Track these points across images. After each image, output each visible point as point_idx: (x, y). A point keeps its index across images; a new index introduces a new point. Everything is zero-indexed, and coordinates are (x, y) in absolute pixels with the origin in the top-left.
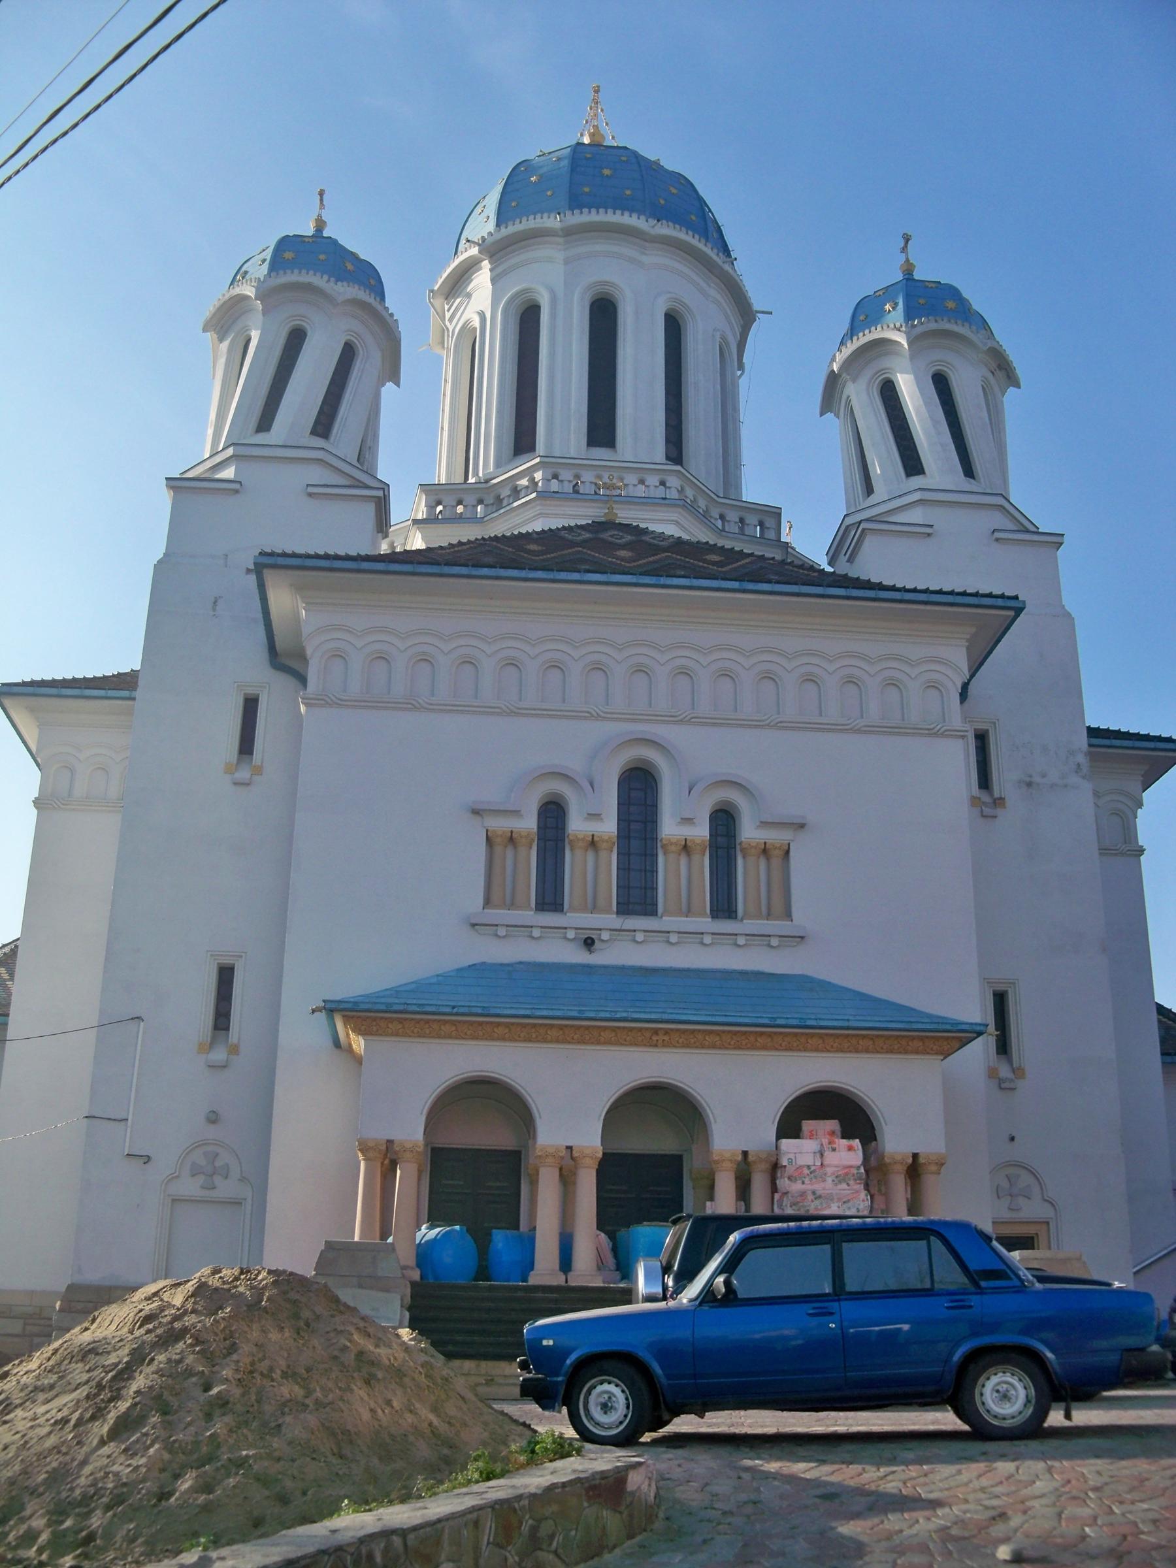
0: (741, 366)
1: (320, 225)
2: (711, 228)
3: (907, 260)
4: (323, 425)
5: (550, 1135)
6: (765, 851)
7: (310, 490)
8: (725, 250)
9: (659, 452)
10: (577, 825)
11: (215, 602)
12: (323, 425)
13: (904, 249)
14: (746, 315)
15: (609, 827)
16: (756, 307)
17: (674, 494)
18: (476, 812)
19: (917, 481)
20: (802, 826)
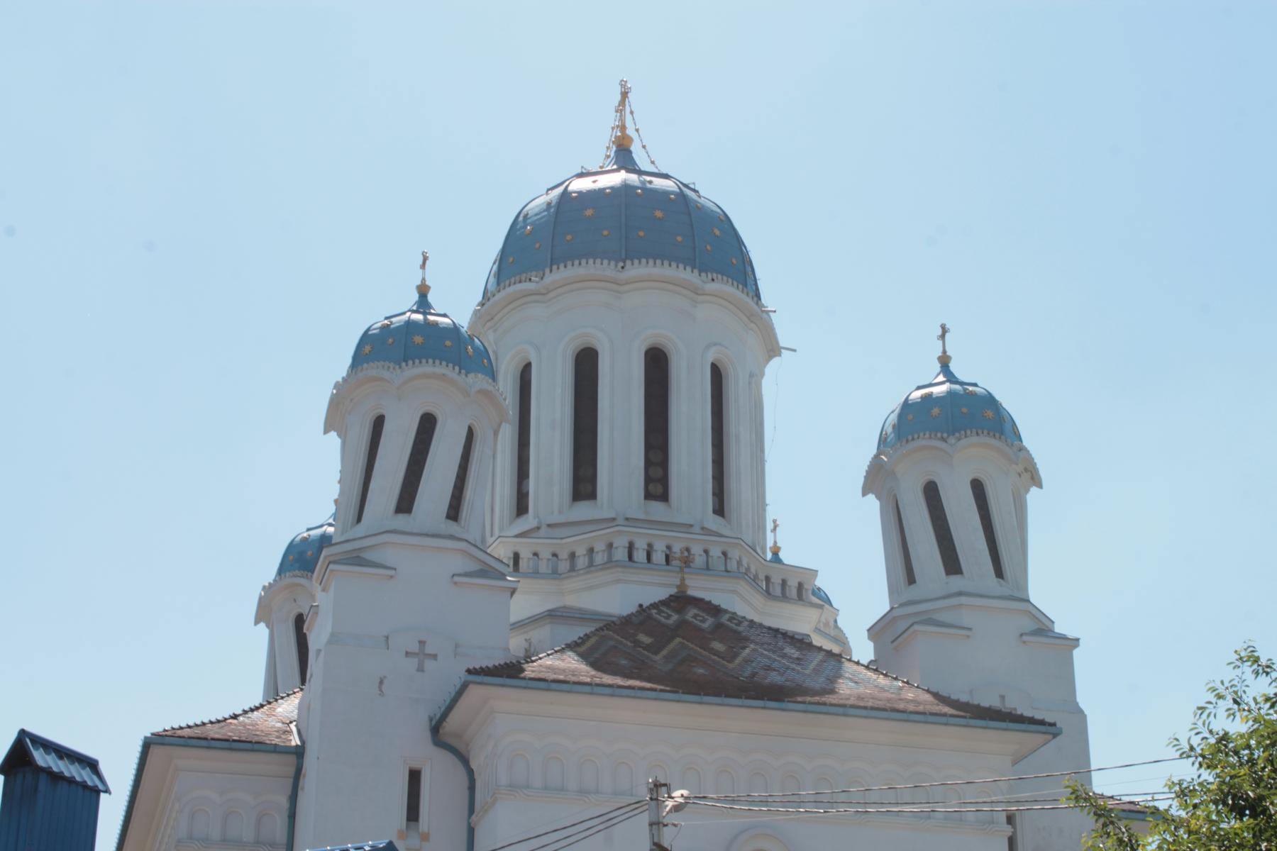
2: (750, 282)
3: (944, 352)
4: (454, 512)
7: (456, 579)
11: (381, 682)
12: (454, 512)
13: (943, 337)
16: (782, 344)
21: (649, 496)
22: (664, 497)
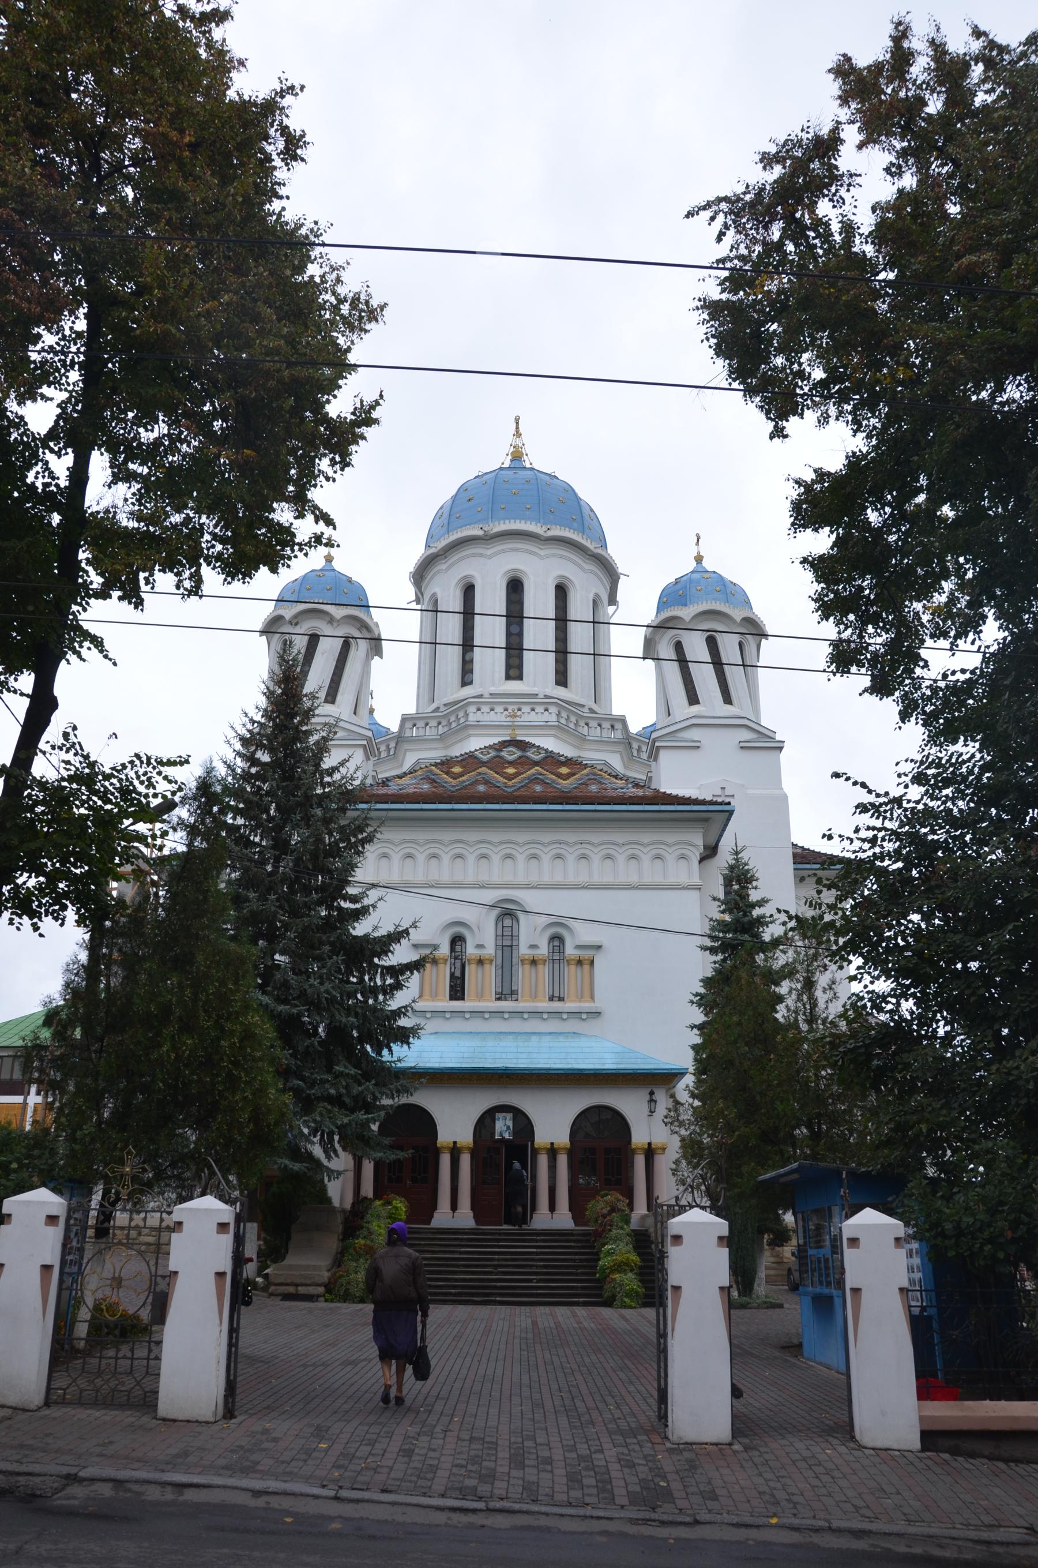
3: (699, 552)
5: (445, 1136)
6: (580, 962)
10: (471, 950)
14: (611, 574)
15: (490, 950)
16: (620, 571)
17: (554, 718)
19: (695, 709)
20: (599, 947)
21: (508, 677)
22: (520, 677)
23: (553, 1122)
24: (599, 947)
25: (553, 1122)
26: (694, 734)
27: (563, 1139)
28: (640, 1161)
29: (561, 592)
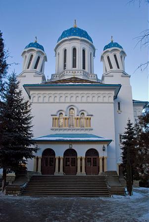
0: (94, 56)
1: (36, 42)
8: (91, 41)
9: (82, 68)
18: (52, 115)
23: (81, 151)
24: (92, 115)
25: (81, 151)
26: (111, 74)
27: (84, 156)
28: (101, 161)
29: (84, 51)
